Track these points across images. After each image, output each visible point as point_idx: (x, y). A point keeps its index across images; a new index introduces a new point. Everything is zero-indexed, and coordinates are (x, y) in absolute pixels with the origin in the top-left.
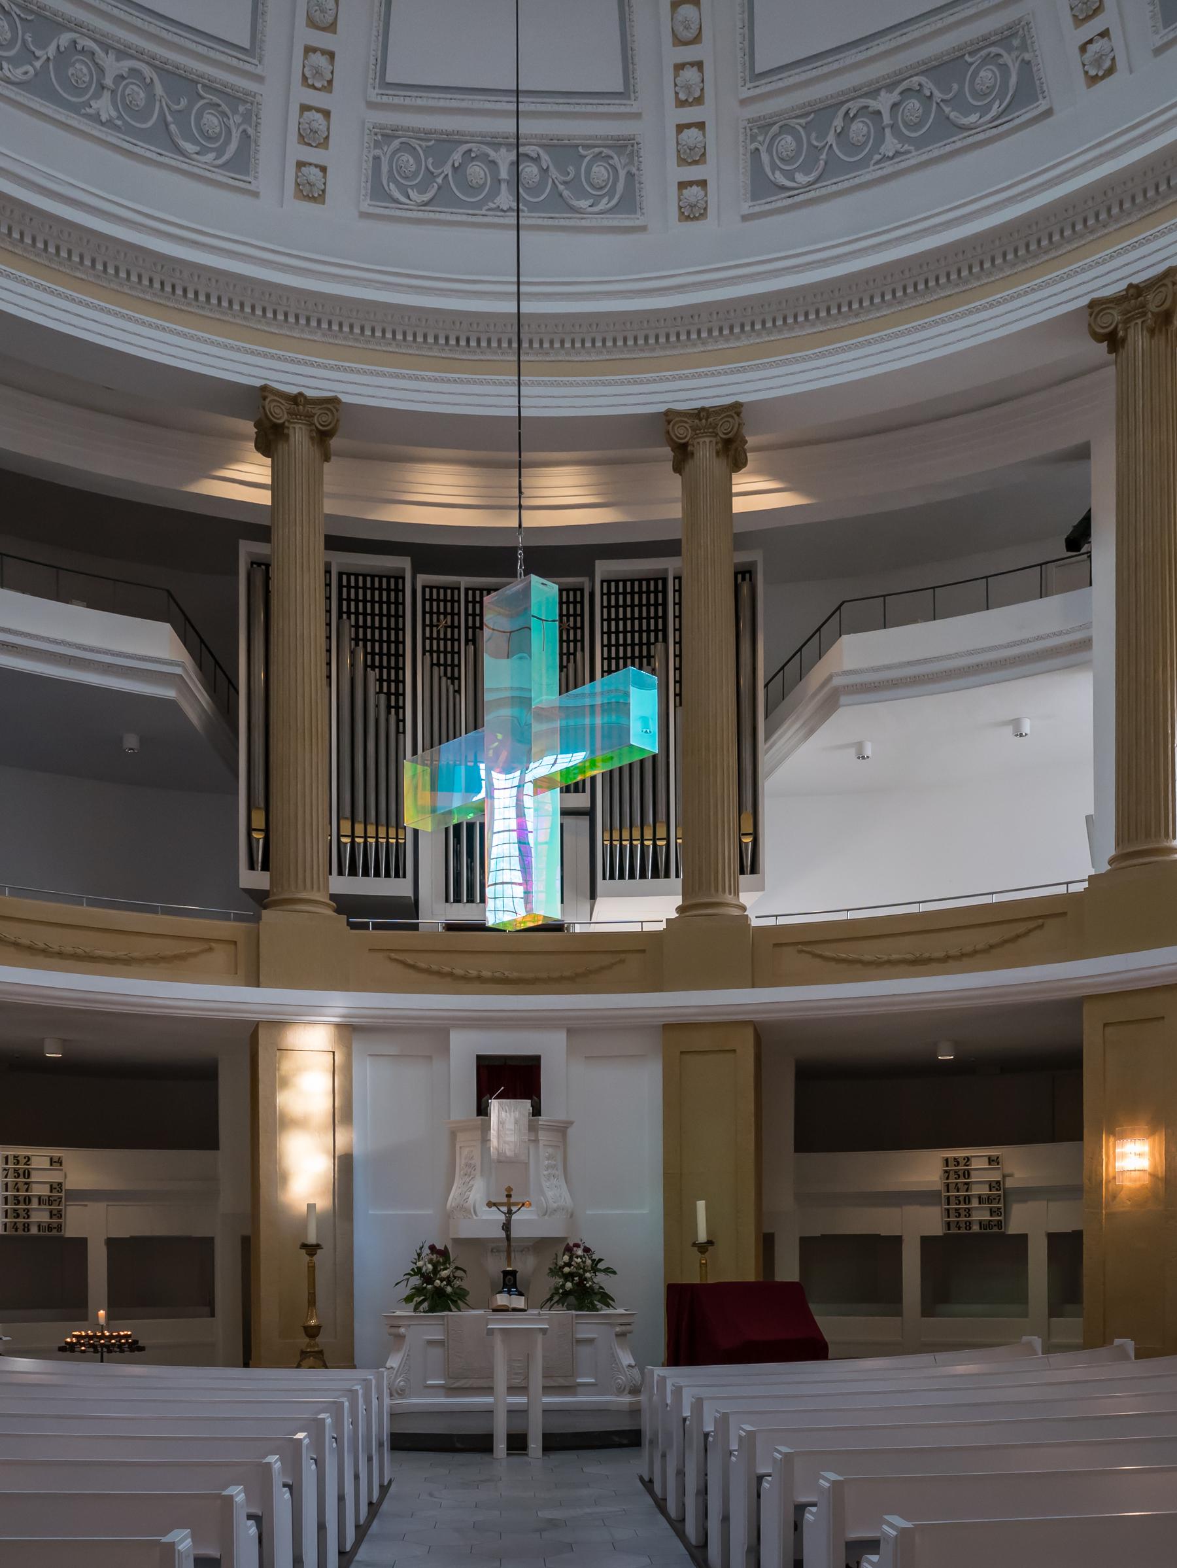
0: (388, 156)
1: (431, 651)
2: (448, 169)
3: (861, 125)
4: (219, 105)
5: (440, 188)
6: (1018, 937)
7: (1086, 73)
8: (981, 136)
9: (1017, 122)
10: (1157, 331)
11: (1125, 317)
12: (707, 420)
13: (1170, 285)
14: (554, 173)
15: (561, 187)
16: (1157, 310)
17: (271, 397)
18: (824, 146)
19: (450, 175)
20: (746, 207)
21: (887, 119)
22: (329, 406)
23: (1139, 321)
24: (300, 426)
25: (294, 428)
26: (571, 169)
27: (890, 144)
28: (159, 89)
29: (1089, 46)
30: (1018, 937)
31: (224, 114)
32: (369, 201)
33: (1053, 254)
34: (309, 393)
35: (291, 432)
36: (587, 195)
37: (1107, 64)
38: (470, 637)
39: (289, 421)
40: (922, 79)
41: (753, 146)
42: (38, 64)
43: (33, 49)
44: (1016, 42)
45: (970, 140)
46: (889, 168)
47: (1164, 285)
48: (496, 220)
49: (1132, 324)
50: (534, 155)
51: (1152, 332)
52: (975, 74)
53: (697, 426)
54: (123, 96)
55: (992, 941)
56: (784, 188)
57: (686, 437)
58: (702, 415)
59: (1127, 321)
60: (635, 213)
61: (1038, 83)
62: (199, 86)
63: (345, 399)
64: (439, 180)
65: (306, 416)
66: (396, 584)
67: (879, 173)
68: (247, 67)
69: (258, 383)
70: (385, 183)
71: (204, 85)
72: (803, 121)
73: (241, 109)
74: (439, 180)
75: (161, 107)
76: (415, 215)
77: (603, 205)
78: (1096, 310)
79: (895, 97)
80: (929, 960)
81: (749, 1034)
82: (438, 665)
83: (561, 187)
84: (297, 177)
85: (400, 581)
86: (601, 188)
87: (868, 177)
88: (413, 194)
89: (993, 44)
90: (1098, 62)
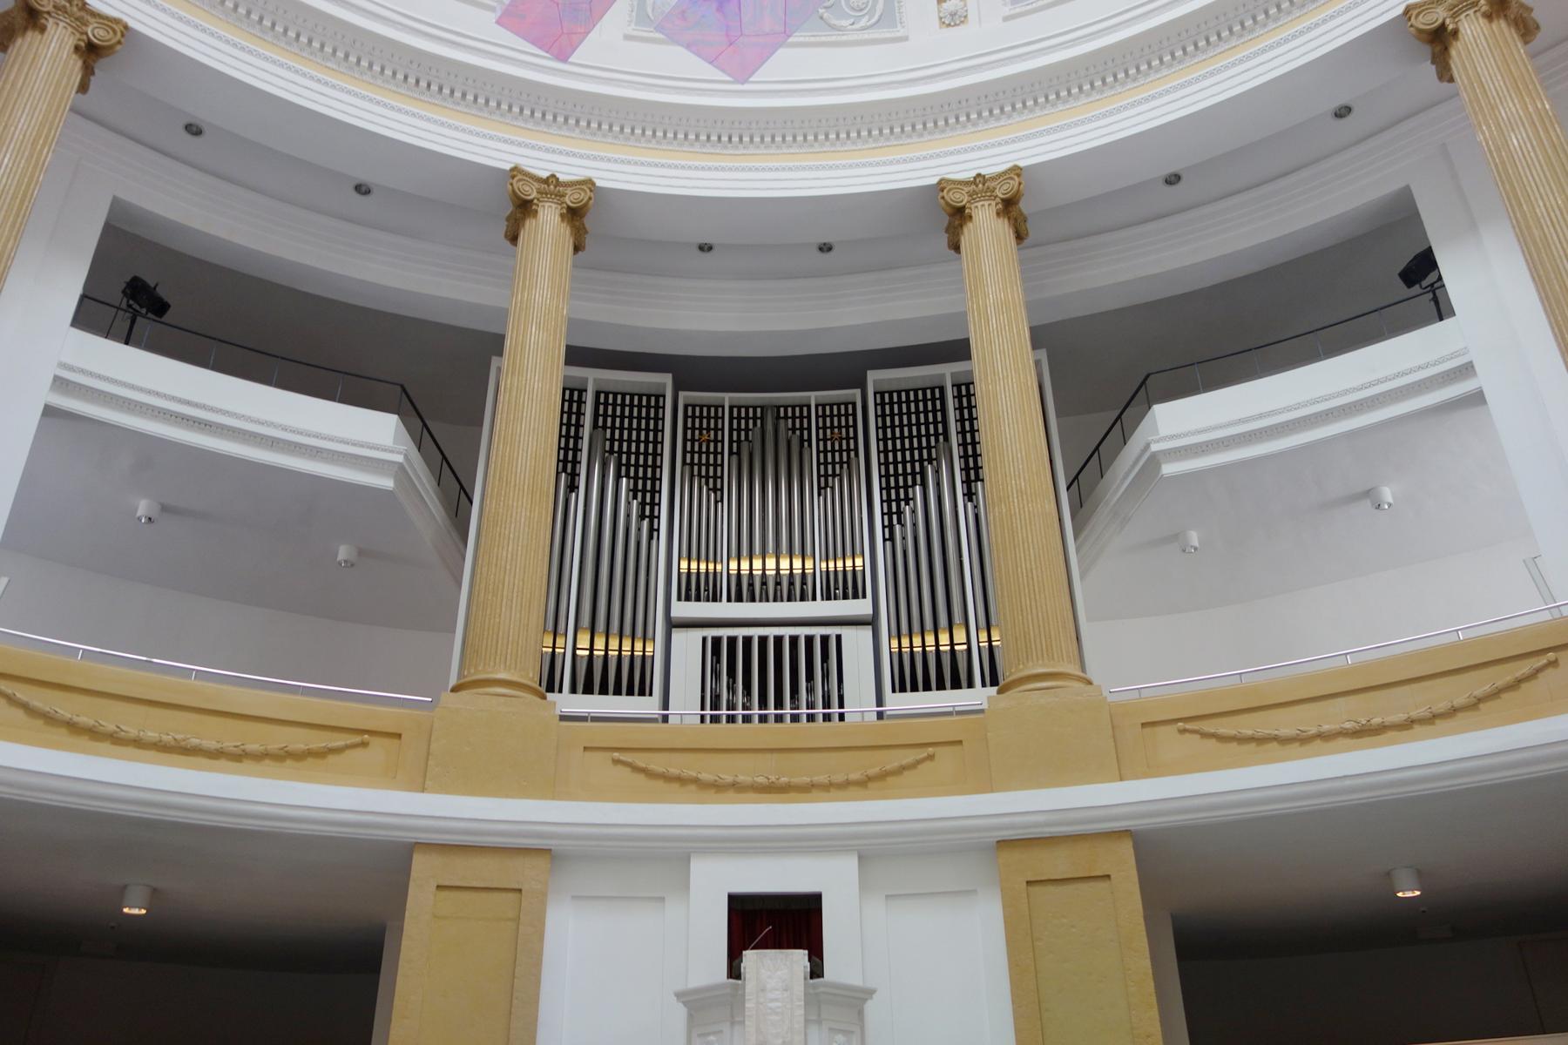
1: (692, 464)
6: (1519, 682)
10: (1494, 15)
11: (1452, 12)
12: (984, 185)
17: (520, 177)
24: (550, 204)
25: (544, 206)
30: (1519, 682)
32: (633, 26)
35: (540, 211)
38: (735, 450)
39: (538, 200)
49: (1463, 16)
53: (974, 191)
55: (1479, 692)
57: (962, 201)
58: (978, 180)
59: (1455, 16)
63: (599, 183)
65: (556, 195)
66: (657, 401)
80: (1382, 729)
81: (1126, 849)
85: (661, 399)
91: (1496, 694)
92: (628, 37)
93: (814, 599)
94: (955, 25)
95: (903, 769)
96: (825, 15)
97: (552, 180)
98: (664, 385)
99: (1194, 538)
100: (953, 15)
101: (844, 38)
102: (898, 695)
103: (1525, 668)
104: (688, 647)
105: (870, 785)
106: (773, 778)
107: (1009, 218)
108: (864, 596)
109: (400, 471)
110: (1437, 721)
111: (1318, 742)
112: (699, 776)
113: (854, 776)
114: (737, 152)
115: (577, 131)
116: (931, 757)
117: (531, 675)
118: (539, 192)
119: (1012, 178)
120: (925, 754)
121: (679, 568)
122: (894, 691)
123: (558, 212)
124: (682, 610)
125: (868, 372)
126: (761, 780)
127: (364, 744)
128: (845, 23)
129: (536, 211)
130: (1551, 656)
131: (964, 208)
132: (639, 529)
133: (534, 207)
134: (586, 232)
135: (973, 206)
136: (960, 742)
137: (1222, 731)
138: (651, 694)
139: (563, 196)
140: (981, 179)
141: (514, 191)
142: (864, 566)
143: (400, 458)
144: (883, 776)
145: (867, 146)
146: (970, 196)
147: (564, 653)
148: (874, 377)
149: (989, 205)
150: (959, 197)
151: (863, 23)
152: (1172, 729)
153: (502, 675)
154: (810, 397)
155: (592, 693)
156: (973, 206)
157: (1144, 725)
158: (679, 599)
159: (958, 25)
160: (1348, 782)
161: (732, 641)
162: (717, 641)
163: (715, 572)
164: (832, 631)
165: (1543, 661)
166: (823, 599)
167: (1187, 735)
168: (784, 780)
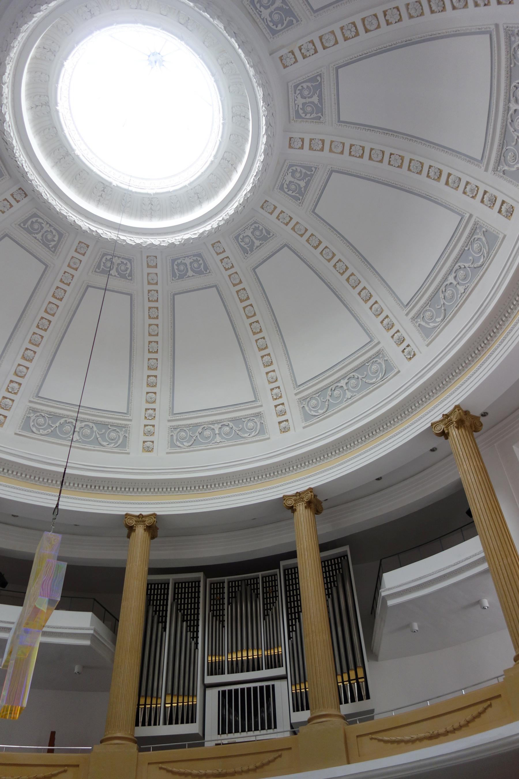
0: (176, 434)
2: (197, 434)
3: (337, 392)
4: (116, 430)
5: (195, 440)
7: (407, 358)
8: (378, 385)
9: (389, 377)
13: (457, 411)
14: (234, 428)
15: (237, 432)
16: (456, 420)
17: (129, 517)
18: (326, 401)
19: (198, 436)
20: (304, 425)
21: (345, 388)
22: (152, 517)
23: (452, 426)
26: (240, 426)
27: (348, 394)
28: (95, 429)
29: (405, 350)
31: (118, 432)
33: (414, 413)
34: (144, 514)
35: (137, 528)
36: (247, 432)
37: (412, 353)
39: (136, 525)
40: (354, 374)
41: (302, 406)
42: (52, 429)
43: (51, 424)
44: (381, 356)
45: (375, 387)
46: (350, 402)
47: (456, 411)
48: (216, 446)
49: (449, 427)
50: (227, 424)
51: (458, 428)
52: (371, 368)
54: (82, 432)
56: (315, 416)
60: (265, 434)
61: (392, 365)
62: (109, 426)
63: (158, 513)
64: (194, 438)
65: (142, 522)
67: (347, 404)
68: (126, 418)
69: (124, 513)
70: (175, 442)
71: (111, 425)
72: (317, 395)
73: (124, 429)
74: (194, 438)
75: (96, 434)
76: (186, 450)
77: (253, 434)
78: (434, 426)
79: (346, 380)
82: (180, 610)
83: (237, 432)
84: (143, 446)
86: (252, 429)
87: (343, 406)
88: (185, 444)
89: (374, 358)
90: (409, 353)
91: (474, 718)
92: (167, 453)
93: (262, 669)
94: (286, 431)
95: (269, 762)
96: (239, 433)
97: (141, 516)
98: (200, 577)
99: (416, 626)
100: (285, 428)
101: (247, 441)
102: (296, 713)
103: (480, 708)
104: (212, 695)
105: (258, 770)
106: (220, 770)
107: (311, 508)
108: (283, 666)
109: (93, 637)
110: (456, 732)
111: (418, 742)
112: (192, 772)
113: (251, 767)
114: (210, 491)
115: (150, 493)
116: (280, 756)
117: (129, 732)
118: (136, 521)
119: (308, 493)
120: (277, 755)
121: (208, 660)
122: (294, 711)
123: (143, 528)
124: (210, 680)
125: (281, 562)
126: (215, 772)
127: (65, 771)
128: (246, 435)
129: (135, 530)
130: (489, 703)
131: (292, 507)
132: (191, 644)
133: (134, 528)
134: (158, 529)
135: (296, 505)
136: (290, 748)
137: (386, 738)
138: (195, 722)
139: (145, 521)
140: (298, 494)
141: (126, 523)
142: (282, 652)
143: (92, 632)
144: (263, 765)
145: (258, 483)
146: (295, 501)
147: (161, 706)
148: (283, 563)
149: (302, 504)
150: (290, 503)
151: (253, 434)
152: (367, 738)
153: (119, 735)
154: (259, 575)
155: (172, 724)
156: (296, 505)
157: (357, 736)
158: (208, 675)
159: (287, 431)
160: (422, 763)
161: (230, 691)
162: (224, 692)
163: (222, 661)
164: (270, 683)
165: (485, 705)
166: (266, 669)
167: (373, 740)
168: (224, 771)
